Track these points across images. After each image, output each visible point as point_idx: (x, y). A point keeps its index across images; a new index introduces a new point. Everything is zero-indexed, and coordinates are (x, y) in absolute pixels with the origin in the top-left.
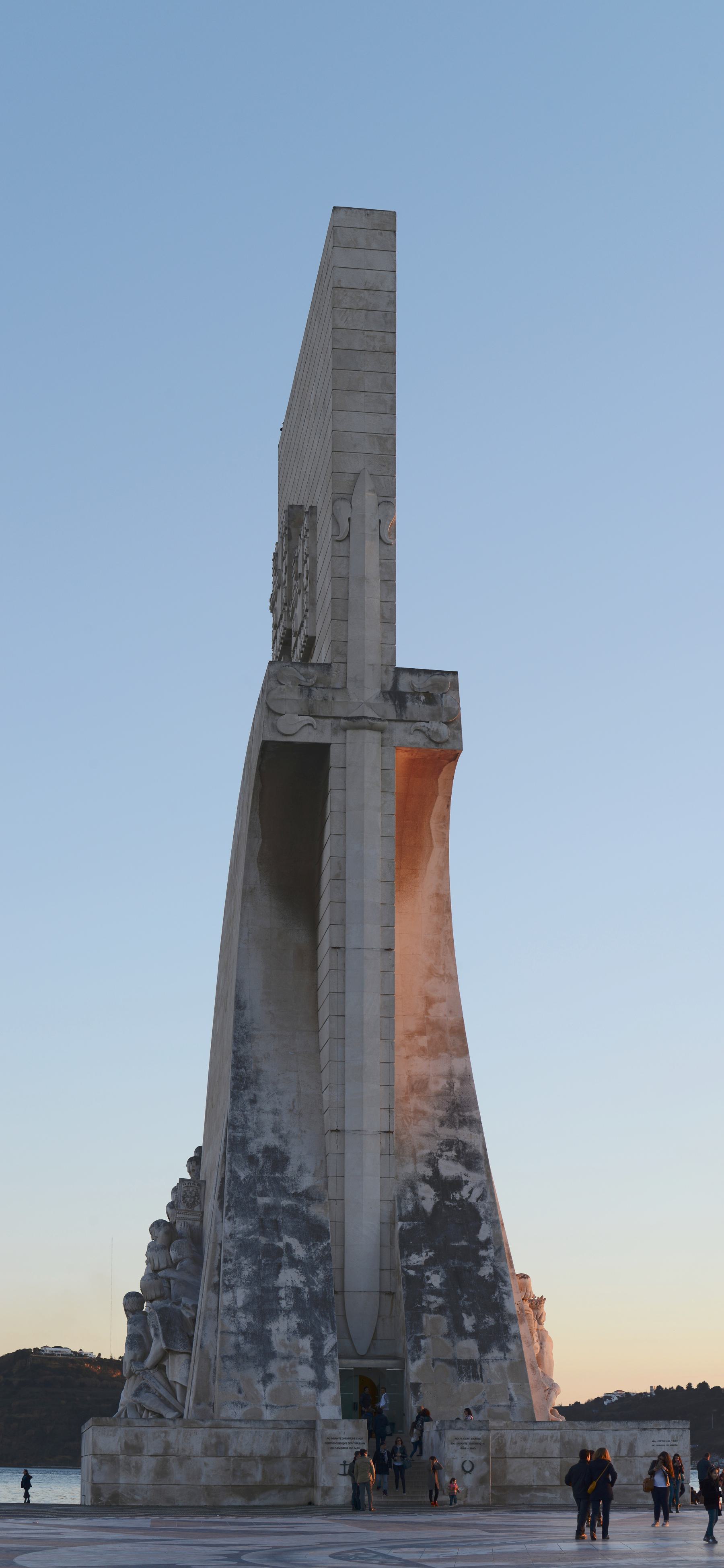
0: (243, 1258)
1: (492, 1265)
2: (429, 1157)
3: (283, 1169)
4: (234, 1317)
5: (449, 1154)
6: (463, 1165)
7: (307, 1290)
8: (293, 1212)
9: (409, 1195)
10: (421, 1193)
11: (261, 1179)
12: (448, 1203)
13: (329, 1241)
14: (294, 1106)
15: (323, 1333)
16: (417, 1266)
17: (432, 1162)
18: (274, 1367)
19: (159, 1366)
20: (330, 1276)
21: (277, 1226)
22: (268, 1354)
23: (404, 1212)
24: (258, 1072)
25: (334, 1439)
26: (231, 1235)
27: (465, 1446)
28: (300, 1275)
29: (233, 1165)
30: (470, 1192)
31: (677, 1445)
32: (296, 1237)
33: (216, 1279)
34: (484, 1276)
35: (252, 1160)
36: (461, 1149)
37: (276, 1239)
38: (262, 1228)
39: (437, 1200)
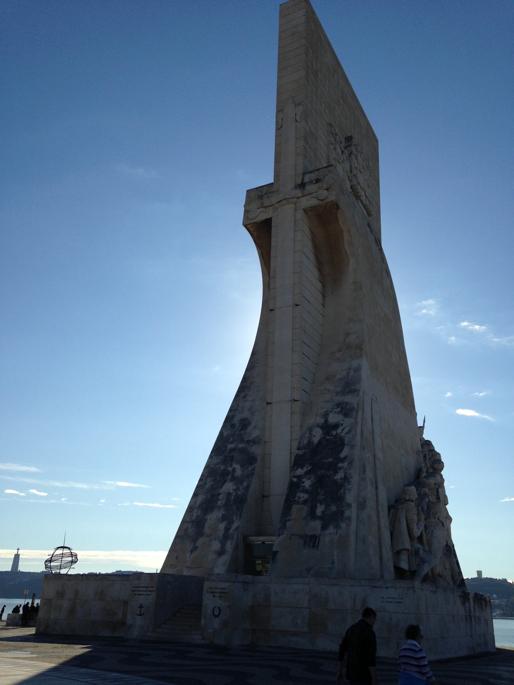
4: (191, 512)
5: (336, 410)
7: (234, 494)
8: (243, 451)
10: (314, 433)
12: (328, 437)
13: (256, 465)
18: (199, 543)
21: (232, 459)
22: (200, 533)
25: (137, 587)
27: (216, 594)
30: (343, 430)
31: (403, 603)
34: (337, 479)
35: (233, 426)
39: (322, 436)
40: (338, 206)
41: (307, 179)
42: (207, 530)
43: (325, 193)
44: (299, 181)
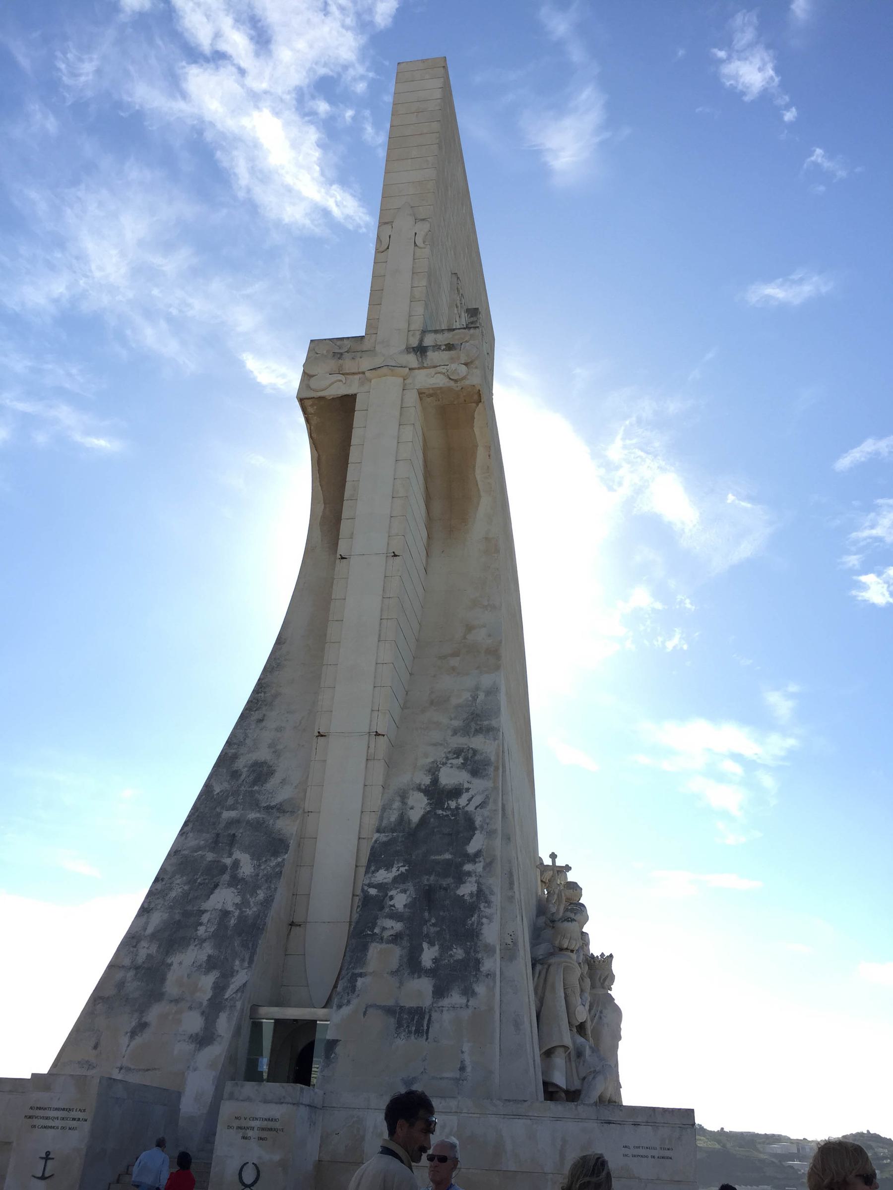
3: (266, 781)
4: (135, 947)
5: (455, 761)
6: (468, 772)
7: (237, 913)
8: (257, 826)
9: (397, 804)
10: (410, 802)
12: (440, 812)
15: (236, 968)
16: (382, 883)
18: (153, 1014)
20: (271, 896)
23: (385, 822)
24: (275, 696)
28: (236, 896)
29: (212, 780)
30: (470, 800)
34: (463, 896)
36: (470, 756)
39: (428, 809)
40: (480, 397)
41: (429, 340)
42: (171, 987)
44: (415, 342)
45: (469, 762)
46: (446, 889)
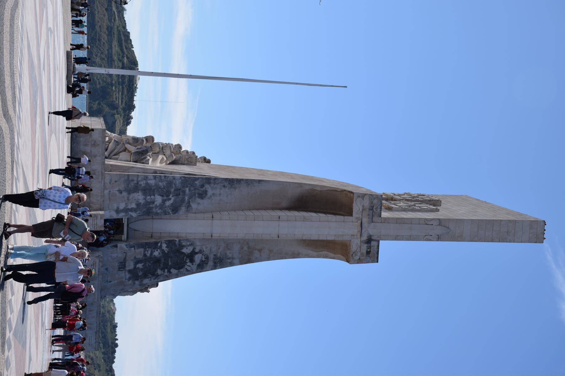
0: (166, 182)
1: (162, 274)
2: (203, 251)
3: (199, 197)
4: (144, 179)
5: (204, 258)
7: (154, 206)
8: (183, 201)
9: (188, 243)
10: (189, 248)
11: (195, 189)
12: (185, 258)
13: (172, 214)
14: (222, 201)
15: (137, 212)
17: (200, 252)
19: (125, 150)
21: (177, 195)
22: (129, 192)
23: (182, 241)
24: (235, 188)
25: (97, 218)
26: (175, 178)
30: (189, 266)
32: (173, 202)
33: (158, 172)
34: (157, 271)
37: (173, 195)
38: (177, 190)
39: (186, 254)
43: (357, 258)
44: (373, 238)
45: (203, 262)
46: (159, 266)
